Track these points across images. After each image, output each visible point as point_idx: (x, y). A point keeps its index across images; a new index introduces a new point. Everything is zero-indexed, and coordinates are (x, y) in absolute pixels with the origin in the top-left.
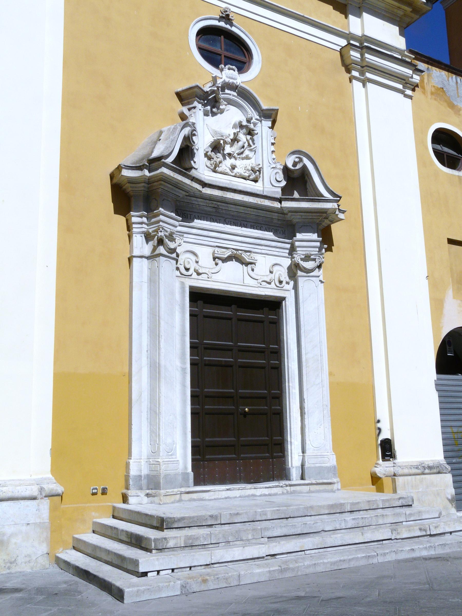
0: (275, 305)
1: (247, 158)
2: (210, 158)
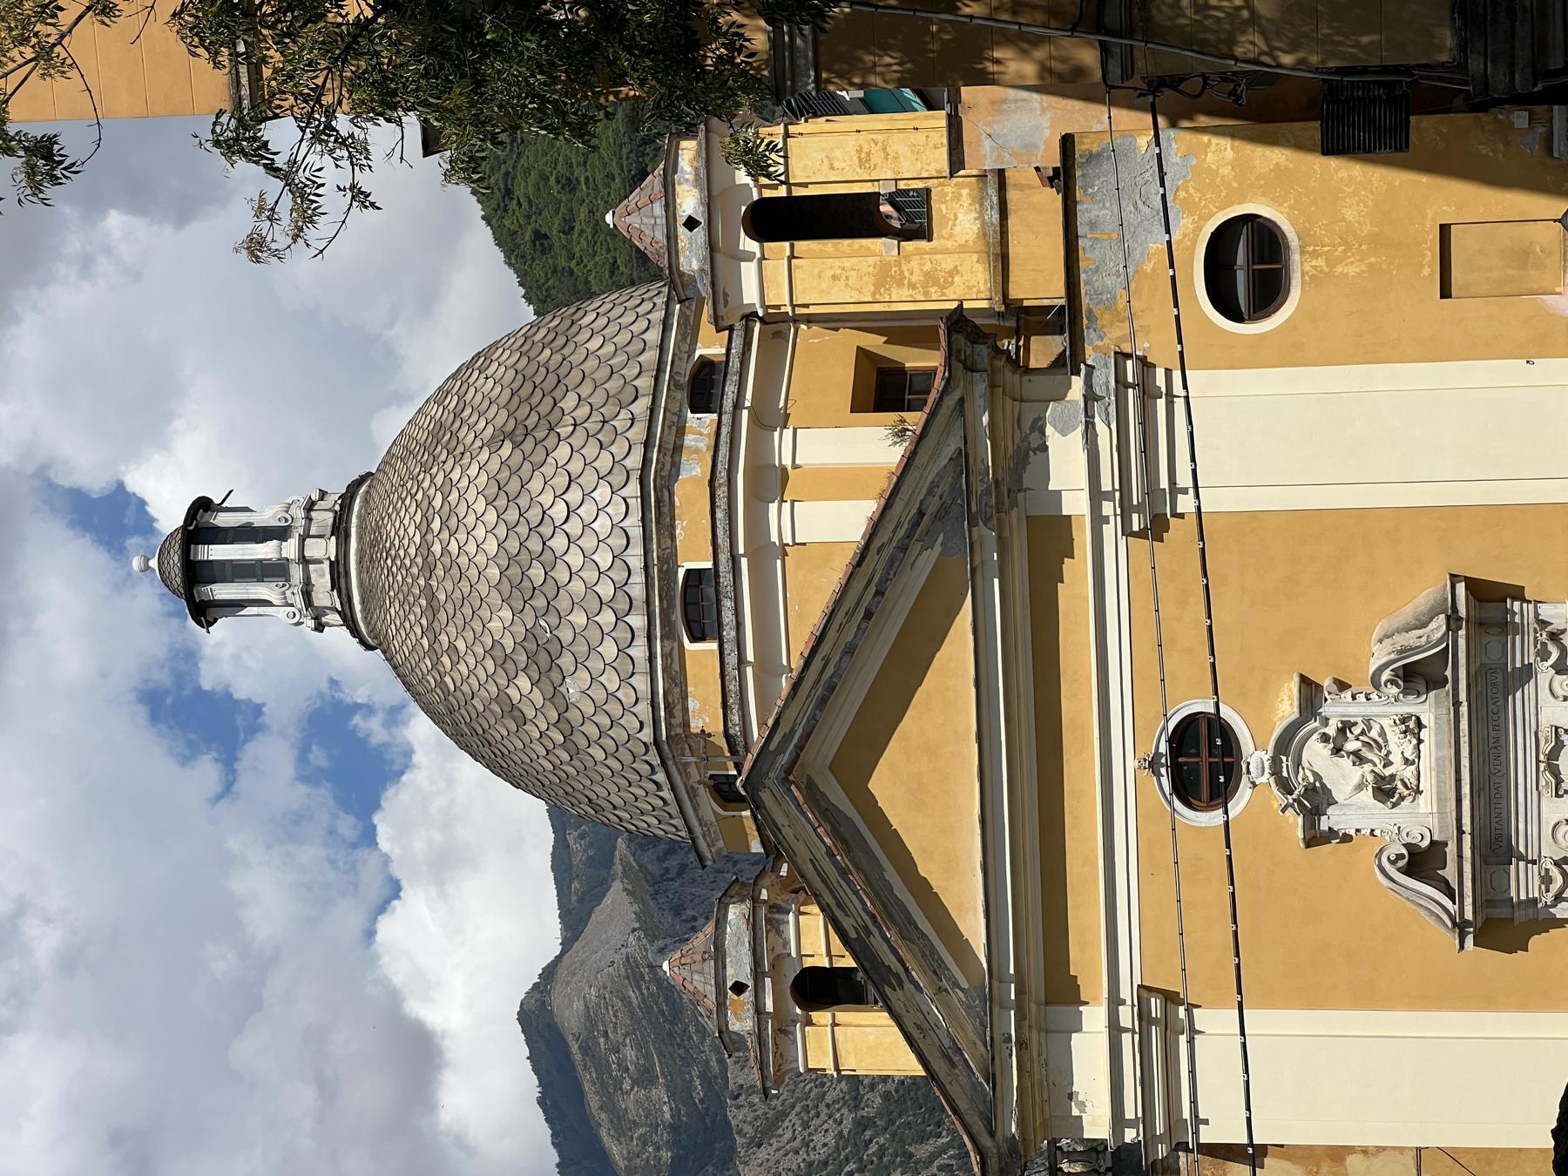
1: (1383, 733)
2: (1402, 798)
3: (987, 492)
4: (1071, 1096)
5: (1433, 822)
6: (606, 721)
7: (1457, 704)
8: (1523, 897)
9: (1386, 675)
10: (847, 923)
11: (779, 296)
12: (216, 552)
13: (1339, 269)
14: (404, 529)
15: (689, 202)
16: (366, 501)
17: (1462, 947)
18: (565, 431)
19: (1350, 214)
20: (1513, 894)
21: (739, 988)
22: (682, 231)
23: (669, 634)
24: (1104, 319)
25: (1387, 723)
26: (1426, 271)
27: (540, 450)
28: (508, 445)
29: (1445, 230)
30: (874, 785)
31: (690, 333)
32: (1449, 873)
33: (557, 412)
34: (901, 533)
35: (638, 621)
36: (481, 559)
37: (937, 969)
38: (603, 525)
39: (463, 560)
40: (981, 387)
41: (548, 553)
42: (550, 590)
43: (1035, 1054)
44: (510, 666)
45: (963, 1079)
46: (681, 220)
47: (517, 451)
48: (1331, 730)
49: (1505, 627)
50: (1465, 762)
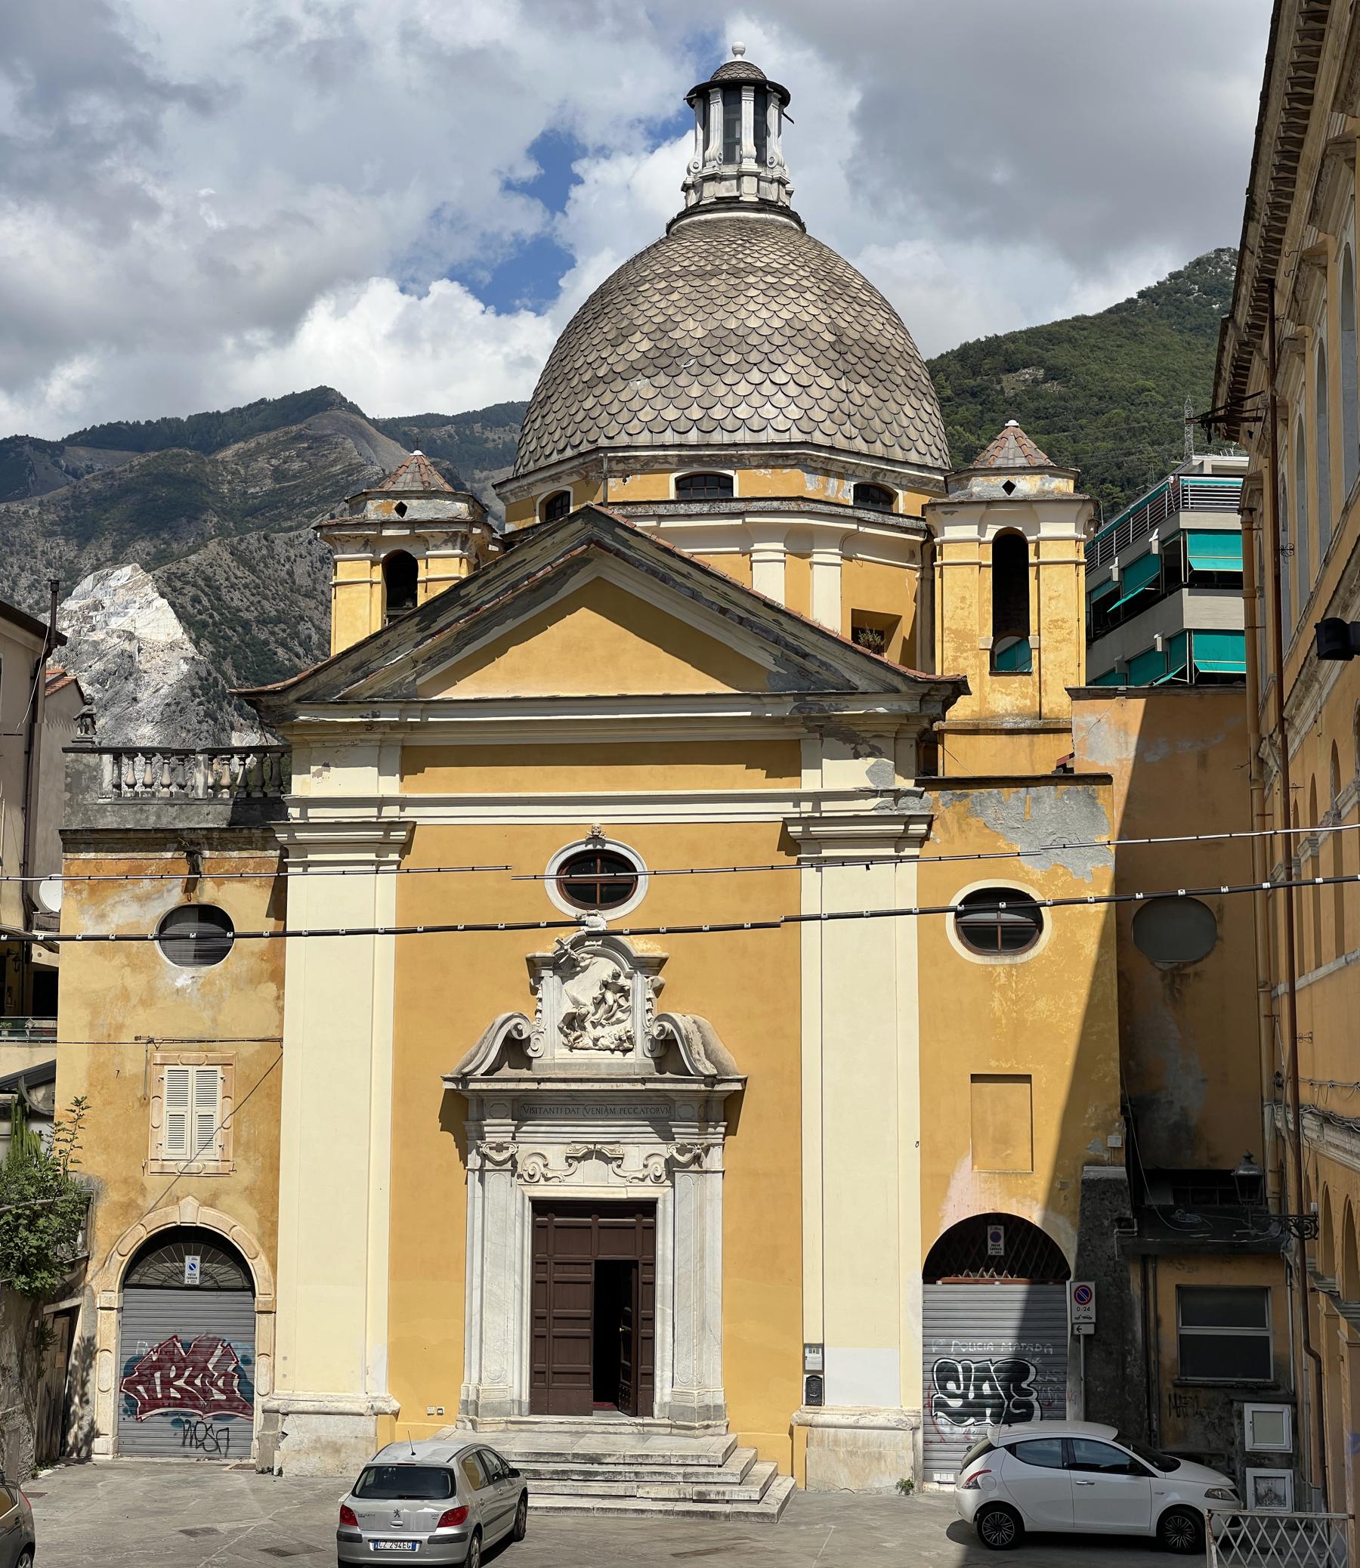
0: (648, 1207)
1: (619, 1021)
2: (566, 1035)
3: (822, 710)
4: (326, 765)
5: (547, 1059)
6: (614, 410)
7: (644, 1081)
8: (486, 1129)
9: (668, 1026)
10: (472, 588)
11: (949, 554)
12: (748, 107)
13: (997, 995)
14: (767, 254)
15: (1027, 486)
16: (786, 226)
17: (446, 1079)
18: (843, 384)
19: (1041, 1004)
20: (488, 1121)
21: (401, 509)
22: (1004, 480)
23: (682, 461)
24: (960, 807)
25: (628, 1025)
26: (993, 1063)
27: (827, 364)
28: (832, 338)
29: (1026, 1078)
30: (584, 613)
31: (916, 486)
32: (506, 1071)
33: (857, 378)
34: (790, 639)
35: (693, 437)
36: (743, 314)
37: (432, 659)
38: (769, 411)
39: (742, 300)
40: (907, 707)
41: (747, 367)
42: (722, 369)
43: (363, 737)
44: (659, 334)
45: (343, 678)
46: (1013, 479)
47: (827, 346)
48: (622, 981)
49: (705, 1120)
50: (596, 1086)
